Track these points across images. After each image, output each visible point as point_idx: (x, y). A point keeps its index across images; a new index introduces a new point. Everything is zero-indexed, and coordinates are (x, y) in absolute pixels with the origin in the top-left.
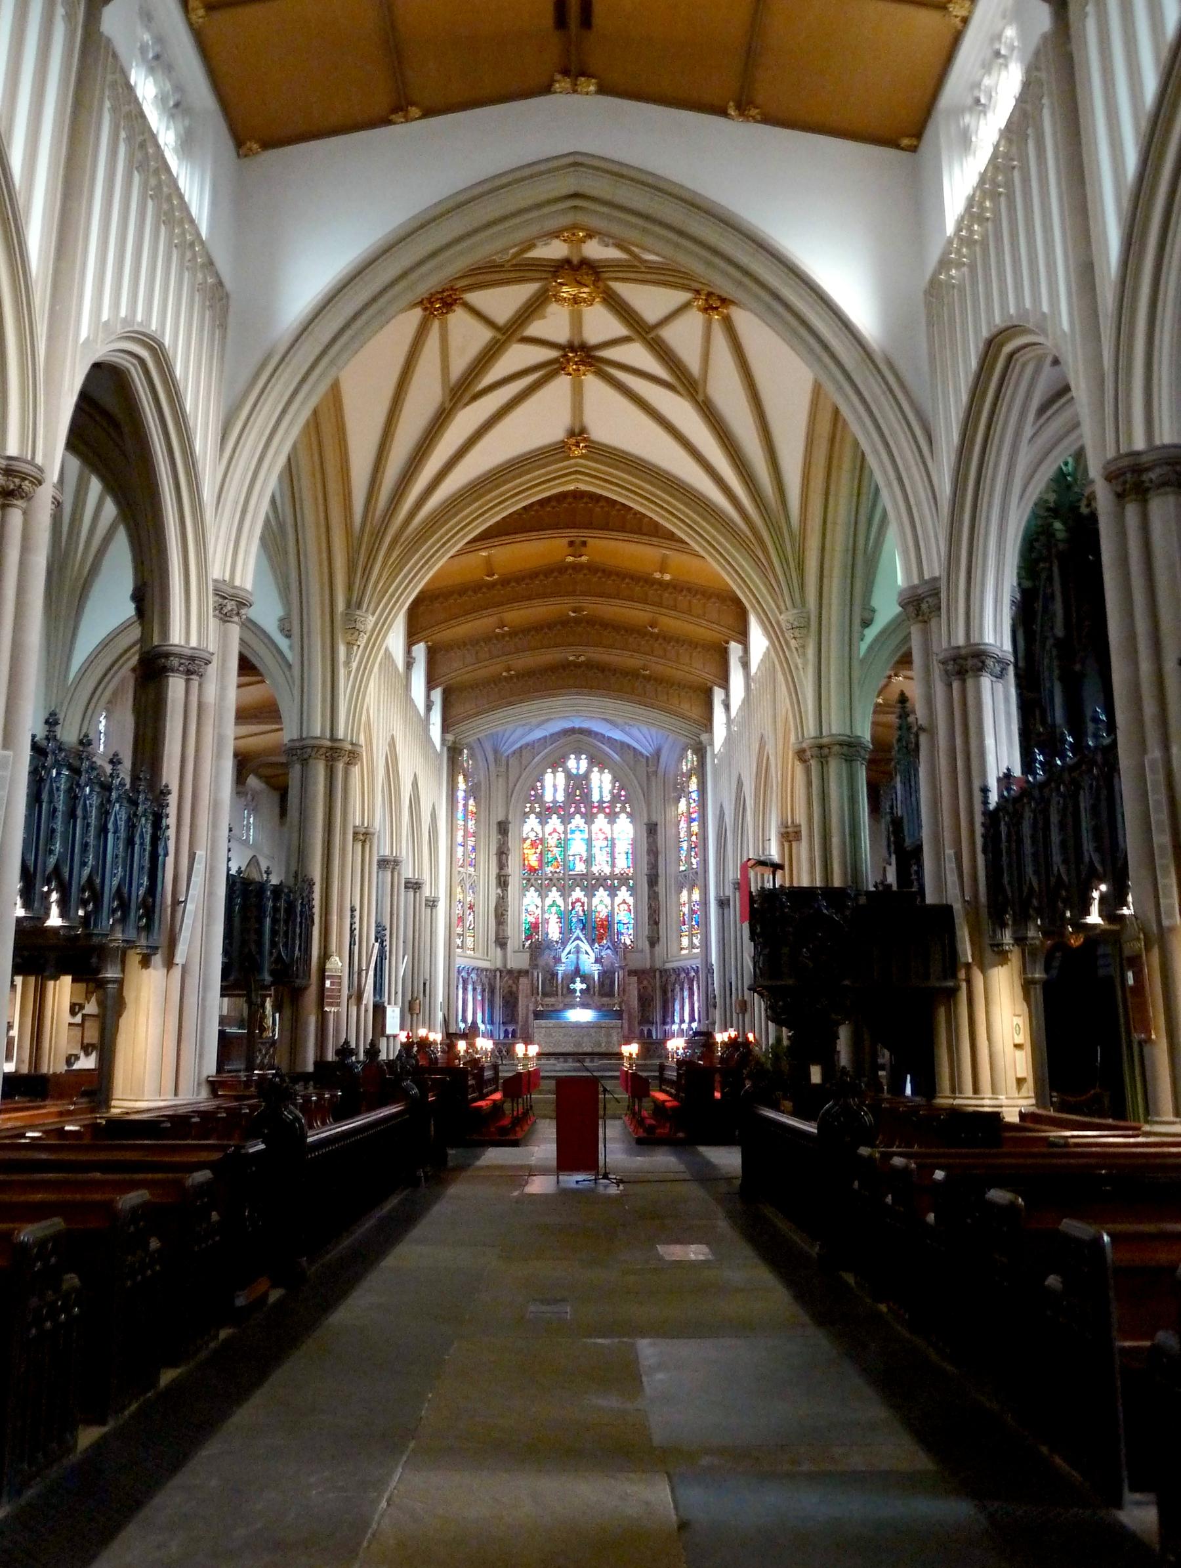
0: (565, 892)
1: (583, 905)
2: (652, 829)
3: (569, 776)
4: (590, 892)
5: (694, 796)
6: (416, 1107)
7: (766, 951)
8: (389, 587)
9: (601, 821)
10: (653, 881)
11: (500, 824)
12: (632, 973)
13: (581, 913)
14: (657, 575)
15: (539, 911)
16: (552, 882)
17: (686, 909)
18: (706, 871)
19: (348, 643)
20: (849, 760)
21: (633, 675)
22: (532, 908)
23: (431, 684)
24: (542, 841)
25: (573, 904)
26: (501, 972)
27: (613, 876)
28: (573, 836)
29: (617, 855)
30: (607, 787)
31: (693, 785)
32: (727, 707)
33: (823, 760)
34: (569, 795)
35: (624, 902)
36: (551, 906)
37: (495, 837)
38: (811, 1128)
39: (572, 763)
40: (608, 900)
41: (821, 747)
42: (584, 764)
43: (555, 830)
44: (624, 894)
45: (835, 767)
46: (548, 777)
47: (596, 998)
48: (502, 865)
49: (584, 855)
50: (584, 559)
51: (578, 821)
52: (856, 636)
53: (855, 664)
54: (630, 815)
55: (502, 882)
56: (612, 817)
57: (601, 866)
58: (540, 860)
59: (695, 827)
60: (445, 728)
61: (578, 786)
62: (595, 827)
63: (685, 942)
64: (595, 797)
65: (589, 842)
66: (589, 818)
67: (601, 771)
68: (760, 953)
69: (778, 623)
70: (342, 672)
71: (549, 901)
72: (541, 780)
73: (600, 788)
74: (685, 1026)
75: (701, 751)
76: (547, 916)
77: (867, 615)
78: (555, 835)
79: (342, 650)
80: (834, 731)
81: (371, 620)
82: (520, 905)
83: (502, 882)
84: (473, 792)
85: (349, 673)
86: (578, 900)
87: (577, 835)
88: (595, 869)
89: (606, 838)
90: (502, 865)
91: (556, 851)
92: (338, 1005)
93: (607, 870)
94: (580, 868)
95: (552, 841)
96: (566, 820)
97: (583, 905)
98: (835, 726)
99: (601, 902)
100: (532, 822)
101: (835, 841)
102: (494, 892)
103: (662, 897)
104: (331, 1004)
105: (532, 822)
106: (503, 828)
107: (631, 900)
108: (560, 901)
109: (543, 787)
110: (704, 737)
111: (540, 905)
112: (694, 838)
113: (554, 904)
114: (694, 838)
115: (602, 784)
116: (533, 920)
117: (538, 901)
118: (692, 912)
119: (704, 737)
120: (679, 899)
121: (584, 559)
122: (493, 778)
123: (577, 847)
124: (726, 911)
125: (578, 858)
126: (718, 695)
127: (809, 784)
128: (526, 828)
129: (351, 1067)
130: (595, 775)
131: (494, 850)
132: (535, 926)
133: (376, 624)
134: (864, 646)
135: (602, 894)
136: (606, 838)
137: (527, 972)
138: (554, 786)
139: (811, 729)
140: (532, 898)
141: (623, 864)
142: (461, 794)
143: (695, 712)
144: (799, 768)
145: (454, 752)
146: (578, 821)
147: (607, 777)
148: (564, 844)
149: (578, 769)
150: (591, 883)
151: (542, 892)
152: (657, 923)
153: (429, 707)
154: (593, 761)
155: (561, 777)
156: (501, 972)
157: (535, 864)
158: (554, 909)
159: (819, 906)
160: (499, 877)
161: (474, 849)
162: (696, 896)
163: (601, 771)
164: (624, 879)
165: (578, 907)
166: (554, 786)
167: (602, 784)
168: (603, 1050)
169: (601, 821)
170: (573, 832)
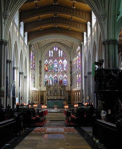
2: (71, 62)
3: (54, 51)
5: (80, 55)
6: (17, 119)
7: (99, 83)
8: (14, 6)
9: (61, 61)
10: (71, 73)
12: (66, 91)
14: (72, 7)
17: (78, 79)
18: (82, 71)
19: (5, 18)
20: (114, 45)
21: (68, 30)
23: (25, 31)
25: (55, 77)
26: (40, 91)
30: (62, 54)
31: (79, 53)
32: (87, 36)
33: (109, 44)
34: (54, 55)
35: (65, 77)
37: (39, 64)
38: (115, 126)
39: (55, 49)
40: (62, 77)
41: (108, 41)
42: (57, 49)
43: (51, 63)
44: (65, 76)
45: (111, 46)
46: (50, 51)
48: (40, 70)
50: (57, 4)
51: (56, 61)
52: (116, 17)
53: (116, 23)
54: (67, 59)
55: (41, 73)
56: (63, 60)
58: (48, 69)
59: (80, 62)
60: (28, 41)
61: (56, 53)
62: (59, 62)
63: (78, 85)
64: (59, 56)
65: (58, 65)
66: (58, 60)
67: (61, 51)
68: (97, 84)
69: (99, 14)
70: (3, 25)
72: (48, 52)
73: (60, 54)
74: (77, 102)
75: (81, 46)
77: (118, 13)
79: (3, 20)
80: (111, 38)
81: (9, 14)
82: (44, 78)
83: (41, 73)
84: (34, 55)
85: (5, 25)
86: (56, 77)
87: (56, 64)
90: (40, 70)
91: (51, 67)
92: (4, 97)
96: (53, 61)
97: (57, 78)
98: (111, 37)
99: (60, 77)
100: (47, 61)
101: (111, 62)
102: (39, 75)
103: (73, 76)
104: (2, 97)
105: (47, 61)
106: (40, 62)
109: (49, 54)
110: (82, 43)
112: (79, 64)
113: (51, 77)
114: (79, 64)
115: (61, 53)
118: (79, 79)
119: (82, 43)
120: (76, 76)
121: (57, 4)
122: (38, 52)
123: (56, 66)
124: (86, 79)
126: (85, 33)
127: (105, 50)
128: (45, 62)
129: (2, 110)
130: (59, 51)
131: (39, 66)
132: (47, 82)
133: (11, 14)
134: (118, 20)
136: (62, 64)
137: (45, 91)
138: (51, 53)
139: (106, 38)
140: (46, 76)
142: (32, 55)
143: (80, 38)
144: (103, 46)
145: (30, 46)
146: (56, 61)
147: (62, 52)
149: (56, 50)
152: (72, 81)
153: (24, 36)
154: (59, 48)
155: (52, 52)
156: (40, 91)
157: (47, 69)
159: (111, 73)
160: (40, 72)
161: (34, 66)
162: (80, 76)
163: (61, 51)
164: (65, 72)
166: (51, 53)
167: (61, 53)
169: (61, 61)
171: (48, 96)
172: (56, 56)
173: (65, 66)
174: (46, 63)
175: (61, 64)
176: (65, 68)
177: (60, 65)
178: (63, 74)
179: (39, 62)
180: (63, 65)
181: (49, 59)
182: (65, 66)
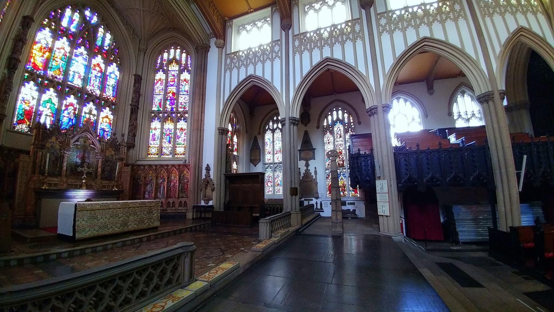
0: (62, 95)
1: (75, 109)
3: (83, 17)
4: (83, 101)
9: (99, 60)
11: (25, 18)
13: (72, 114)
15: (34, 103)
16: (53, 83)
22: (28, 98)
24: (51, 50)
25: (67, 106)
27: (100, 98)
28: (77, 58)
29: (107, 87)
30: (107, 42)
35: (107, 117)
36: (48, 102)
47: (99, 180)
49: (83, 74)
51: (82, 50)
54: (120, 68)
57: (94, 87)
64: (99, 43)
65: (88, 68)
71: (45, 97)
76: (41, 108)
78: (62, 51)
86: (72, 105)
87: (80, 59)
88: (89, 88)
89: (101, 72)
91: (62, 64)
93: (98, 92)
94: (78, 83)
95: (59, 54)
96: (74, 45)
107: (111, 117)
108: (55, 100)
111: (36, 97)
113: (50, 101)
116: (28, 108)
117: (36, 94)
125: (77, 75)
130: (101, 30)
131: (13, 35)
135: (91, 105)
136: (101, 72)
141: (109, 93)
148: (69, 62)
150: (84, 96)
151: (42, 89)
157: (40, 64)
158: (48, 105)
165: (71, 108)
168: (145, 226)
169: (99, 60)
170: (76, 56)
171: (42, 173)
172: (84, 37)
173: (111, 82)
174: (43, 42)
175: (98, 69)
176: (111, 88)
177: (95, 73)
178: (100, 108)
179: (19, 19)
180: (104, 78)
181: (59, 33)
182: (111, 82)
